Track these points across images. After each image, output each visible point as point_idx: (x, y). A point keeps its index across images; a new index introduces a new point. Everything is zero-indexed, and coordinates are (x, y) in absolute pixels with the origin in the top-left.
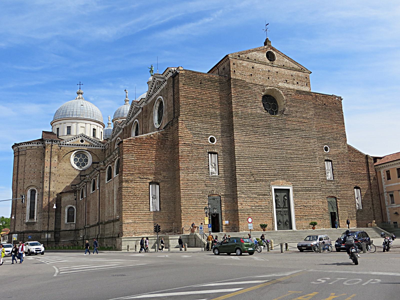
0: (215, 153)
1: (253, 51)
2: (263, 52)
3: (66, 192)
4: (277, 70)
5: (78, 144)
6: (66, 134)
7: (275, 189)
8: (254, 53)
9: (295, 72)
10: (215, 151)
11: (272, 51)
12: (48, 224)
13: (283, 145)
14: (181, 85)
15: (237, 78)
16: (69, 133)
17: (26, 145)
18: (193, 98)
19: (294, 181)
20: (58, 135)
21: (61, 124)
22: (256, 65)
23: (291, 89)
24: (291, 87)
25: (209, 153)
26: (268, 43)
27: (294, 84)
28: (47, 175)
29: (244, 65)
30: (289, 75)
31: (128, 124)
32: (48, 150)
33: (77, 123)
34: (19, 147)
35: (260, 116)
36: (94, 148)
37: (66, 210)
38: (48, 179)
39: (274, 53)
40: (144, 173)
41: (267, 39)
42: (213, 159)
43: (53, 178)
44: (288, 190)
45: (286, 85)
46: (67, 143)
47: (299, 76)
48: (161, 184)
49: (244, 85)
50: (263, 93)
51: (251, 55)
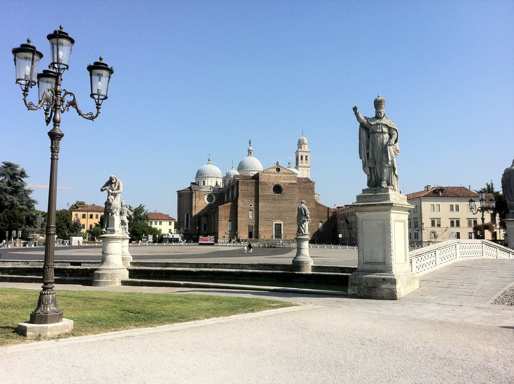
0: (252, 210)
1: (270, 169)
2: (275, 168)
3: (203, 216)
4: (281, 175)
5: (209, 191)
6: (202, 185)
7: (275, 224)
8: (270, 169)
9: (289, 175)
10: (252, 209)
11: (279, 167)
12: (195, 231)
13: (280, 206)
14: (239, 186)
15: (262, 181)
16: (204, 184)
17: (183, 192)
18: (244, 190)
19: (284, 220)
20: (198, 185)
21: (200, 179)
22: (271, 175)
23: (286, 183)
24: (287, 182)
25: (249, 210)
26: (278, 164)
27: (288, 180)
28: (194, 207)
29: (265, 175)
30: (286, 177)
31: (229, 188)
32: (194, 195)
33: (208, 179)
34: (180, 192)
35: (271, 195)
36: (217, 192)
37: (203, 225)
38: (194, 209)
39: (280, 168)
40: (226, 218)
41: (278, 162)
42: (250, 212)
43: (197, 209)
44: (281, 224)
45: (284, 181)
46: (203, 191)
47: (291, 177)
48: (232, 221)
49: (265, 184)
50: (273, 186)
51: (269, 171)
